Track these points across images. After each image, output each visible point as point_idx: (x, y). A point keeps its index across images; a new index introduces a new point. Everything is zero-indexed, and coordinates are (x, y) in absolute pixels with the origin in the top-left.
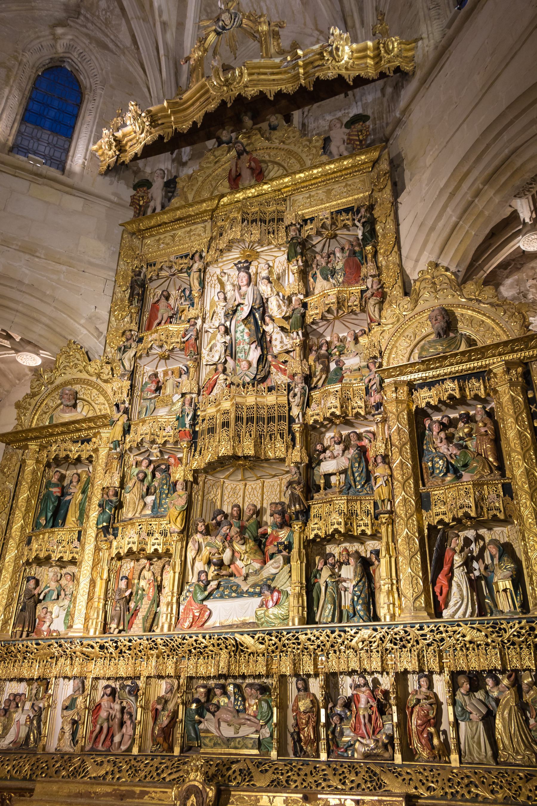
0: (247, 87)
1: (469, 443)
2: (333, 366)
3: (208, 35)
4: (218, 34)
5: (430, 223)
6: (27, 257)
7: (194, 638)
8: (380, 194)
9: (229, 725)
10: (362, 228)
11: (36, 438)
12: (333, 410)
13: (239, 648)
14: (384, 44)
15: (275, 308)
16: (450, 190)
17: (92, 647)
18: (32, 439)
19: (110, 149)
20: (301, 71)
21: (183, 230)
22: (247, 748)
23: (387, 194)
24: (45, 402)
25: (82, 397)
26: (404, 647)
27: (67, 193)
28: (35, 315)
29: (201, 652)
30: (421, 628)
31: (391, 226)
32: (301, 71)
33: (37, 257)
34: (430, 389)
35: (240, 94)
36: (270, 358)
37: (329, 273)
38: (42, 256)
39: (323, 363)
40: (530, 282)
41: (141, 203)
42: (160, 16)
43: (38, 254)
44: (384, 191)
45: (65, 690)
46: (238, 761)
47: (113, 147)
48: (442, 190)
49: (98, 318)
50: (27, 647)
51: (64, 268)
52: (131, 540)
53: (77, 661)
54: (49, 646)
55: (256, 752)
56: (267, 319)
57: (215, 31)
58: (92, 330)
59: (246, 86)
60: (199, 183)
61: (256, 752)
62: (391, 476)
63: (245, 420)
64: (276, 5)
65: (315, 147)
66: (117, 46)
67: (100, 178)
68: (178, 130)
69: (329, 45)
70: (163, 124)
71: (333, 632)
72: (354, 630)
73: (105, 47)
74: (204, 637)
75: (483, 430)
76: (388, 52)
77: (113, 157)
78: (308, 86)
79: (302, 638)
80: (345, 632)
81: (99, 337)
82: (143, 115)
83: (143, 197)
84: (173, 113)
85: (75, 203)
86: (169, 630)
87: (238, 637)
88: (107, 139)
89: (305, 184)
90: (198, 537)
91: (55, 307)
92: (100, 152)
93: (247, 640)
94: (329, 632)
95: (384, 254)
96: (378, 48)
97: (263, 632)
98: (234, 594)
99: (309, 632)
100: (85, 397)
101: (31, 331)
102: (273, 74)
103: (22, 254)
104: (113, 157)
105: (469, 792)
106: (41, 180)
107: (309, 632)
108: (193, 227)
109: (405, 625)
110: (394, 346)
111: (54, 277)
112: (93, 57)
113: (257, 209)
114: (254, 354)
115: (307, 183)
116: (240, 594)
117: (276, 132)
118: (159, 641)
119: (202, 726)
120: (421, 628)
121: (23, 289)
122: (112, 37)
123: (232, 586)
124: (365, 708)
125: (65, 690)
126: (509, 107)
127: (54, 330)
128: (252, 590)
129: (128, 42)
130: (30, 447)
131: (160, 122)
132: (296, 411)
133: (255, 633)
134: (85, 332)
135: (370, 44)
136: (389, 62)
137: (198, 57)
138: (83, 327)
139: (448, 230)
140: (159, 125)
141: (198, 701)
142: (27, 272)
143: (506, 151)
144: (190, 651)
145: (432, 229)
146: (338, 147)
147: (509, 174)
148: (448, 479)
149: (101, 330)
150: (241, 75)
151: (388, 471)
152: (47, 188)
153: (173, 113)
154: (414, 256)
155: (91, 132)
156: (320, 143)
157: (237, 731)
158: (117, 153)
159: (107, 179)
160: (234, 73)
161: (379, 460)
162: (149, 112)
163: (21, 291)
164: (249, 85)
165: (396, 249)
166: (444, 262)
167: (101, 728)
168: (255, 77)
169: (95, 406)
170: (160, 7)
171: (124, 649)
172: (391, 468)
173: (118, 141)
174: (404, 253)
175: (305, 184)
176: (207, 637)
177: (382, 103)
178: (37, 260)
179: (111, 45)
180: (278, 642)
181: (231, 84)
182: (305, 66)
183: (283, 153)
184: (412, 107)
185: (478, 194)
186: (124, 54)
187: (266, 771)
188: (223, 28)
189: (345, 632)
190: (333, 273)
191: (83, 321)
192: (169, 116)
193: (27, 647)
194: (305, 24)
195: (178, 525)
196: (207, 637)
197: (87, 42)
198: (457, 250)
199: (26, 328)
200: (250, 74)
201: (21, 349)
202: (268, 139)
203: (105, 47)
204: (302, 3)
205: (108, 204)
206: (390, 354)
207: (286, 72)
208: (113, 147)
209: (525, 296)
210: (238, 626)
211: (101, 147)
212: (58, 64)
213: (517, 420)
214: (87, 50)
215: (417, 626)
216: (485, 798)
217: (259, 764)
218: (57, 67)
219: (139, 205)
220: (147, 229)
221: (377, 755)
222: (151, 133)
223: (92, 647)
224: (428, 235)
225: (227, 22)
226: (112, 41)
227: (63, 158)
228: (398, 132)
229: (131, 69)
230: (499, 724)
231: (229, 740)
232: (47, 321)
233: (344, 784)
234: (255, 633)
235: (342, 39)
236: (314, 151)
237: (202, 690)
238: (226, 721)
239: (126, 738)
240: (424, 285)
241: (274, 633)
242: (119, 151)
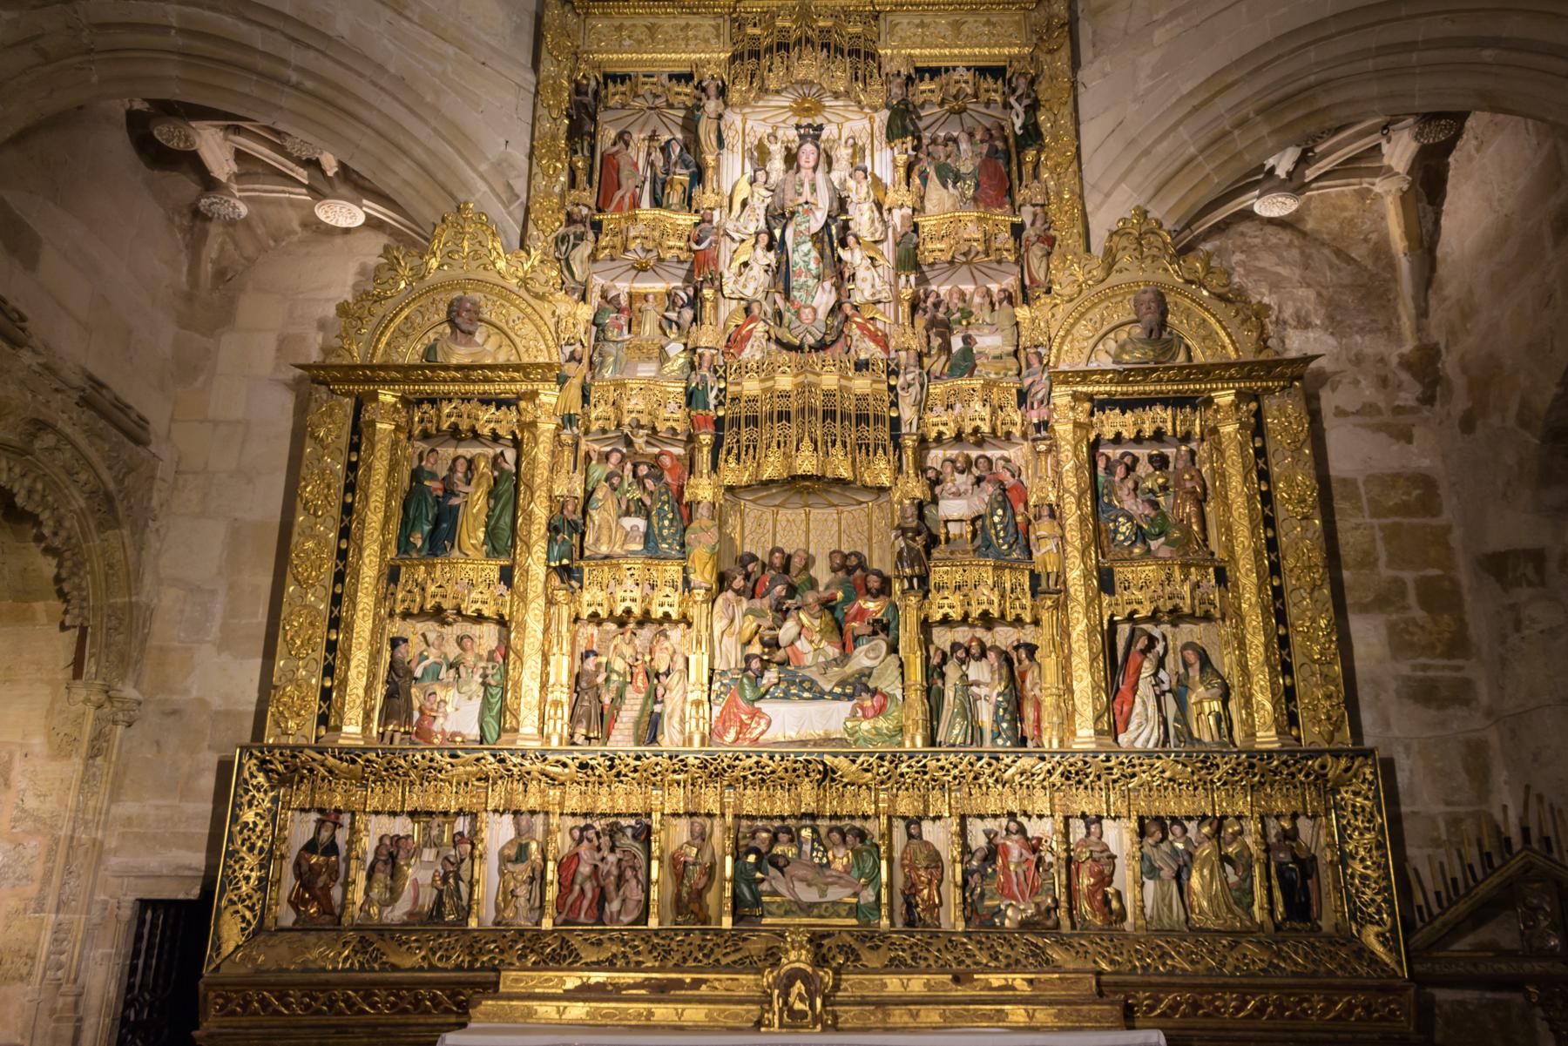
2: (957, 344)
7: (755, 759)
8: (1049, 58)
9: (809, 885)
10: (1022, 115)
11: (393, 381)
12: (979, 422)
13: (828, 773)
15: (862, 218)
16: (1195, 102)
17: (565, 765)
18: (384, 382)
21: (673, 22)
22: (839, 916)
23: (1062, 61)
25: (487, 316)
26: (1079, 782)
30: (1108, 759)
31: (1065, 121)
34: (1123, 413)
36: (847, 309)
37: (949, 175)
39: (939, 334)
40: (1238, 257)
44: (1057, 56)
45: (498, 833)
46: (829, 935)
48: (1182, 98)
49: (511, 166)
50: (432, 760)
51: (451, 50)
52: (628, 595)
53: (533, 787)
54: (478, 760)
55: (854, 922)
56: (851, 240)
58: (500, 189)
61: (854, 922)
62: (1062, 538)
63: (820, 414)
71: (979, 759)
72: (1012, 757)
74: (772, 758)
75: (1189, 485)
80: (998, 759)
81: (511, 202)
86: (703, 744)
87: (828, 759)
90: (730, 594)
91: (435, 130)
93: (842, 763)
94: (973, 758)
95: (1052, 171)
97: (871, 754)
98: (806, 695)
99: (942, 756)
100: (494, 318)
101: (388, 168)
105: (1164, 964)
107: (942, 756)
108: (694, 21)
109: (1085, 753)
110: (1068, 332)
113: (829, 24)
114: (824, 298)
116: (820, 695)
118: (691, 760)
119: (764, 887)
120: (1108, 759)
124: (1018, 864)
125: (498, 833)
126: (1337, 16)
127: (432, 176)
128: (838, 690)
130: (381, 397)
132: (907, 413)
133: (857, 755)
138: (482, 177)
139: (1177, 164)
141: (756, 851)
143: (1312, 78)
144: (745, 778)
145: (1146, 152)
147: (1301, 112)
148: (1137, 551)
149: (517, 190)
151: (1057, 529)
154: (1106, 187)
157: (823, 894)
161: (1045, 512)
165: (1075, 166)
166: (1154, 213)
167: (582, 890)
169: (517, 340)
171: (624, 771)
174: (1090, 175)
176: (777, 757)
180: (889, 769)
185: (1241, 124)
187: (878, 947)
189: (998, 759)
190: (958, 177)
191: (483, 167)
193: (432, 760)
195: (707, 576)
196: (777, 757)
198: (1182, 199)
199: (380, 161)
201: (327, 190)
206: (1061, 344)
210: (816, 744)
213: (1245, 479)
215: (1102, 757)
216: (1184, 970)
217: (862, 939)
221: (1037, 923)
223: (565, 765)
224: (1137, 160)
230: (1195, 882)
231: (812, 905)
233: (996, 959)
234: (857, 755)
237: (765, 835)
239: (631, 905)
240: (1124, 242)
241: (888, 757)
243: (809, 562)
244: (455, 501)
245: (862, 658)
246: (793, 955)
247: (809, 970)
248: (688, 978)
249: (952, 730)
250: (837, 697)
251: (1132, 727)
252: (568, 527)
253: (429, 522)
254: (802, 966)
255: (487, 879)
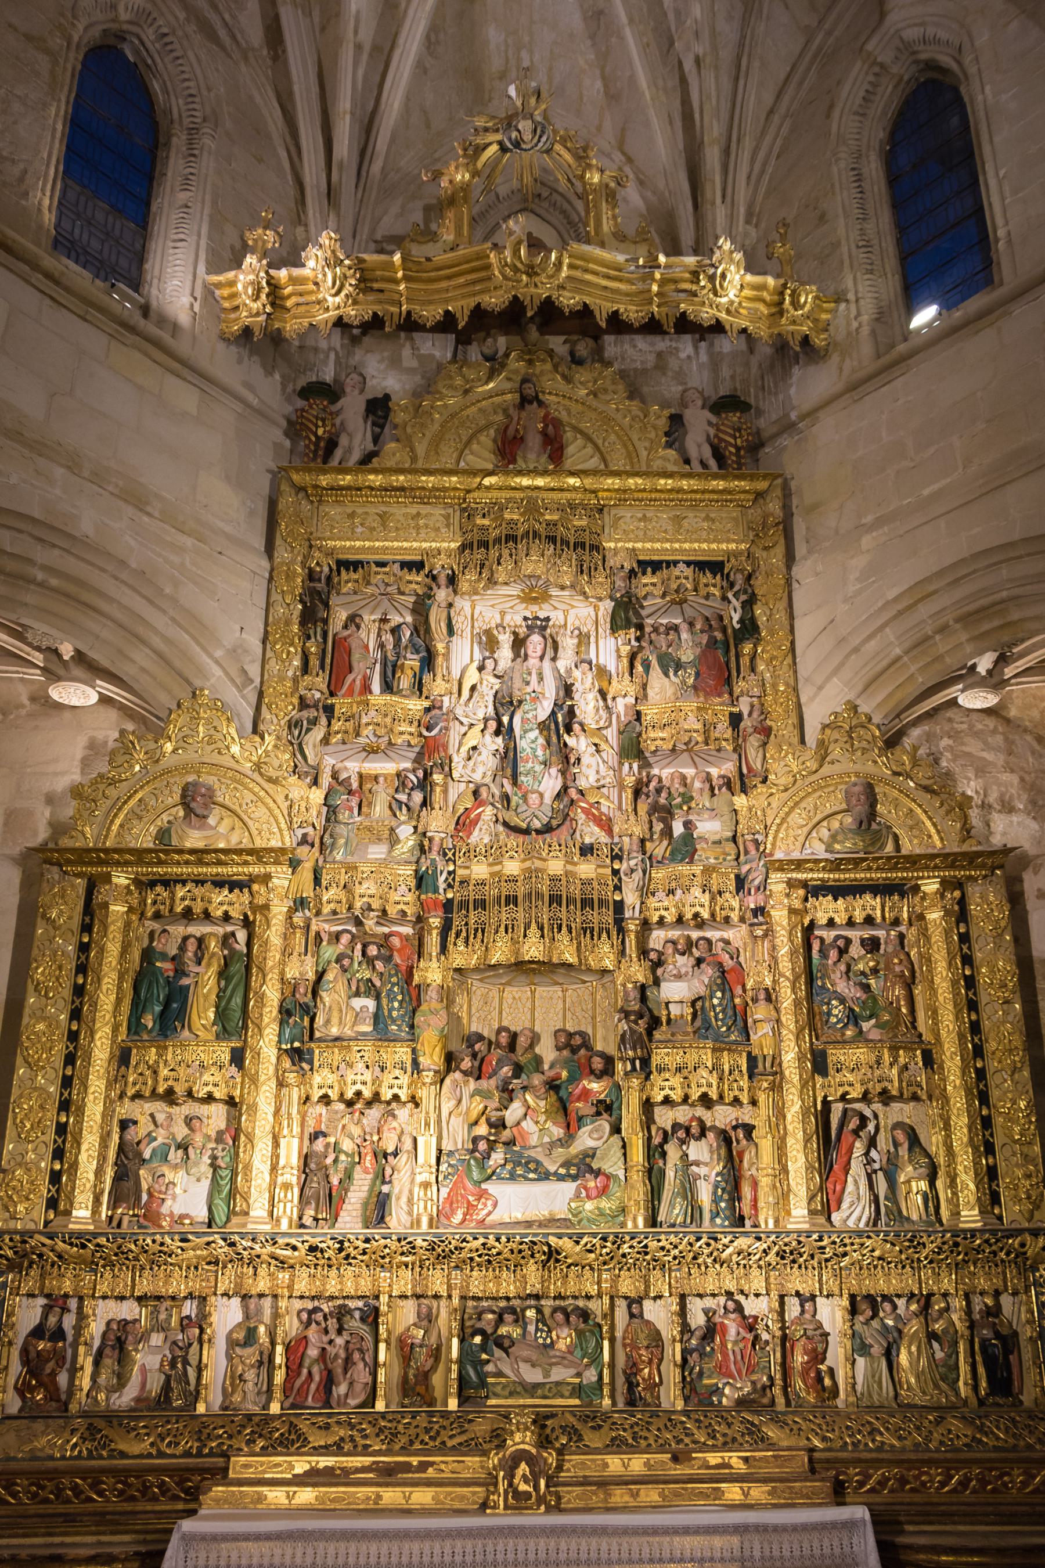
0: (564, 288)
1: (872, 982)
2: (678, 828)
3: (487, 146)
4: (503, 149)
5: (856, 641)
6: (130, 511)
7: (482, 1240)
8: (765, 554)
9: (533, 1366)
10: (739, 610)
11: (127, 863)
12: (698, 909)
13: (552, 1254)
14: (794, 292)
15: (587, 706)
16: (900, 607)
17: (294, 1248)
18: (118, 864)
19: (256, 298)
20: (655, 288)
21: (404, 510)
22: (562, 1396)
23: (776, 558)
24: (138, 796)
25: (220, 799)
26: (794, 1261)
27: (172, 372)
28: (140, 630)
29: (489, 1260)
30: (821, 1239)
31: (781, 616)
32: (655, 288)
33: (148, 514)
34: (836, 899)
35: (549, 297)
36: (573, 793)
37: (670, 664)
38: (156, 514)
39: (661, 820)
40: (945, 742)
41: (320, 432)
42: (356, 32)
43: (149, 509)
44: (772, 552)
45: (226, 1316)
46: (553, 1416)
47: (263, 296)
48: (888, 603)
49: (246, 651)
50: (162, 1244)
51: (189, 542)
52: (359, 1078)
53: (263, 1271)
54: (208, 1244)
55: (577, 1402)
56: (576, 727)
57: (500, 143)
58: (234, 673)
59: (561, 287)
60: (436, 426)
61: (577, 1402)
62: (778, 1021)
63: (546, 898)
64: (550, 69)
65: (654, 427)
66: (234, 37)
67: (221, 346)
68: (414, 316)
69: (712, 265)
70: (381, 291)
71: (698, 1239)
72: (729, 1238)
73: (211, 35)
74: (498, 1240)
75: (897, 969)
76: (796, 304)
77: (258, 314)
78: (664, 321)
79: (653, 1245)
80: (716, 1239)
81: (244, 686)
82: (347, 262)
83: (323, 420)
84: (406, 278)
85: (185, 397)
86: (431, 1226)
87: (553, 1240)
88: (252, 277)
89: (640, 495)
90: (457, 1075)
91: (173, 619)
92: (226, 292)
93: (566, 1244)
94: (693, 1239)
95: (769, 662)
96: (782, 294)
97: (594, 1235)
98: (531, 1176)
99: (663, 1237)
100: (227, 802)
101: (127, 658)
102: (608, 277)
103: (120, 503)
104: (258, 314)
105: (873, 1441)
106: (132, 338)
107: (663, 1237)
108: (425, 510)
109: (799, 1233)
110: (783, 820)
111: (175, 559)
112: (190, 54)
113: (556, 517)
114: (551, 783)
115: (645, 495)
116: (545, 1176)
117: (580, 369)
118: (419, 1242)
119: (490, 1368)
120: (821, 1239)
121: (124, 576)
122: (227, 16)
123: (527, 1163)
124: (735, 1343)
125: (226, 1316)
126: (1024, 540)
127: (167, 662)
128: (562, 1171)
129: (254, 34)
130: (115, 880)
131: (376, 286)
132: (630, 897)
133: (581, 1236)
134: (218, 672)
135: (771, 281)
136: (794, 322)
137: (462, 182)
138: (217, 662)
139: (885, 663)
140: (372, 289)
141: (482, 1332)
142: (132, 543)
143: (1004, 594)
144: (472, 1259)
145: (856, 650)
146: (699, 446)
147: (996, 623)
148: (849, 1033)
149: (251, 675)
150: (559, 264)
151: (773, 1013)
152: (137, 355)
153: (406, 278)
154: (819, 680)
155: (199, 236)
156: (663, 423)
157: (547, 1374)
158: (268, 309)
159: (233, 349)
160: (547, 257)
161: (762, 996)
162: (361, 261)
163: (116, 578)
164: (568, 286)
165: (789, 660)
166: (864, 708)
167: (310, 1373)
168: (577, 274)
169: (250, 823)
170: (358, 12)
171: (353, 1253)
172: (777, 1010)
173: (274, 287)
174: (803, 670)
175: (640, 495)
176: (504, 1239)
177: (747, 365)
178: (146, 519)
179: (222, 33)
180: (612, 1250)
181: (537, 274)
182: (662, 283)
183: (593, 415)
184: (821, 414)
185: (943, 629)
186: (246, 59)
187: (600, 1427)
188: (517, 144)
189: (716, 1239)
190: (679, 666)
191: (219, 653)
192: (397, 282)
193: (162, 1244)
194: (599, 128)
195: (436, 1058)
196: (504, 1239)
197: (182, 15)
198: (890, 695)
199: (120, 652)
200: (571, 266)
201: (61, 672)
202: (568, 380)
203: (211, 35)
204: (606, 93)
205: (239, 407)
206: (777, 832)
207: (629, 281)
208: (263, 296)
209: (936, 761)
210: (541, 1224)
211: (232, 283)
212: (112, 41)
213: (950, 964)
214: (180, 33)
215: (815, 1236)
217: (585, 1419)
218: (109, 46)
219: (315, 434)
220: (332, 489)
221: (753, 1401)
222: (355, 302)
223: (294, 1248)
224: (847, 656)
225: (527, 136)
226: (226, 24)
227: (66, 225)
228: (785, 441)
229: (258, 99)
230: (904, 1358)
231: (536, 1386)
232: (161, 646)
233: (714, 1438)
234: (581, 1236)
235: (732, 260)
236: (653, 435)
237: (490, 1316)
238: (526, 1361)
239: (358, 1387)
240: (836, 735)
241: (611, 1238)
242: (273, 304)
243: (535, 1039)
244: (185, 981)
245: (586, 1139)
246: (518, 1437)
247: (534, 1451)
248: (415, 1461)
249: (672, 1210)
250: (561, 1178)
251: (845, 1205)
252: (299, 1010)
253: (159, 1003)
254: (527, 1447)
255: (215, 1360)
